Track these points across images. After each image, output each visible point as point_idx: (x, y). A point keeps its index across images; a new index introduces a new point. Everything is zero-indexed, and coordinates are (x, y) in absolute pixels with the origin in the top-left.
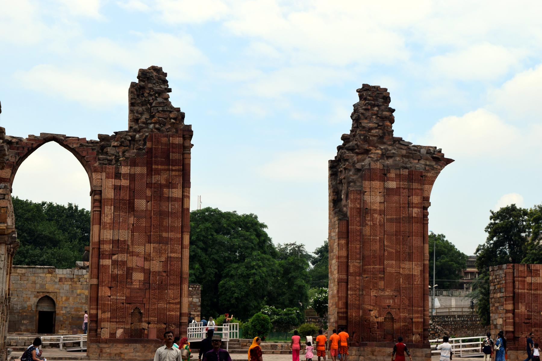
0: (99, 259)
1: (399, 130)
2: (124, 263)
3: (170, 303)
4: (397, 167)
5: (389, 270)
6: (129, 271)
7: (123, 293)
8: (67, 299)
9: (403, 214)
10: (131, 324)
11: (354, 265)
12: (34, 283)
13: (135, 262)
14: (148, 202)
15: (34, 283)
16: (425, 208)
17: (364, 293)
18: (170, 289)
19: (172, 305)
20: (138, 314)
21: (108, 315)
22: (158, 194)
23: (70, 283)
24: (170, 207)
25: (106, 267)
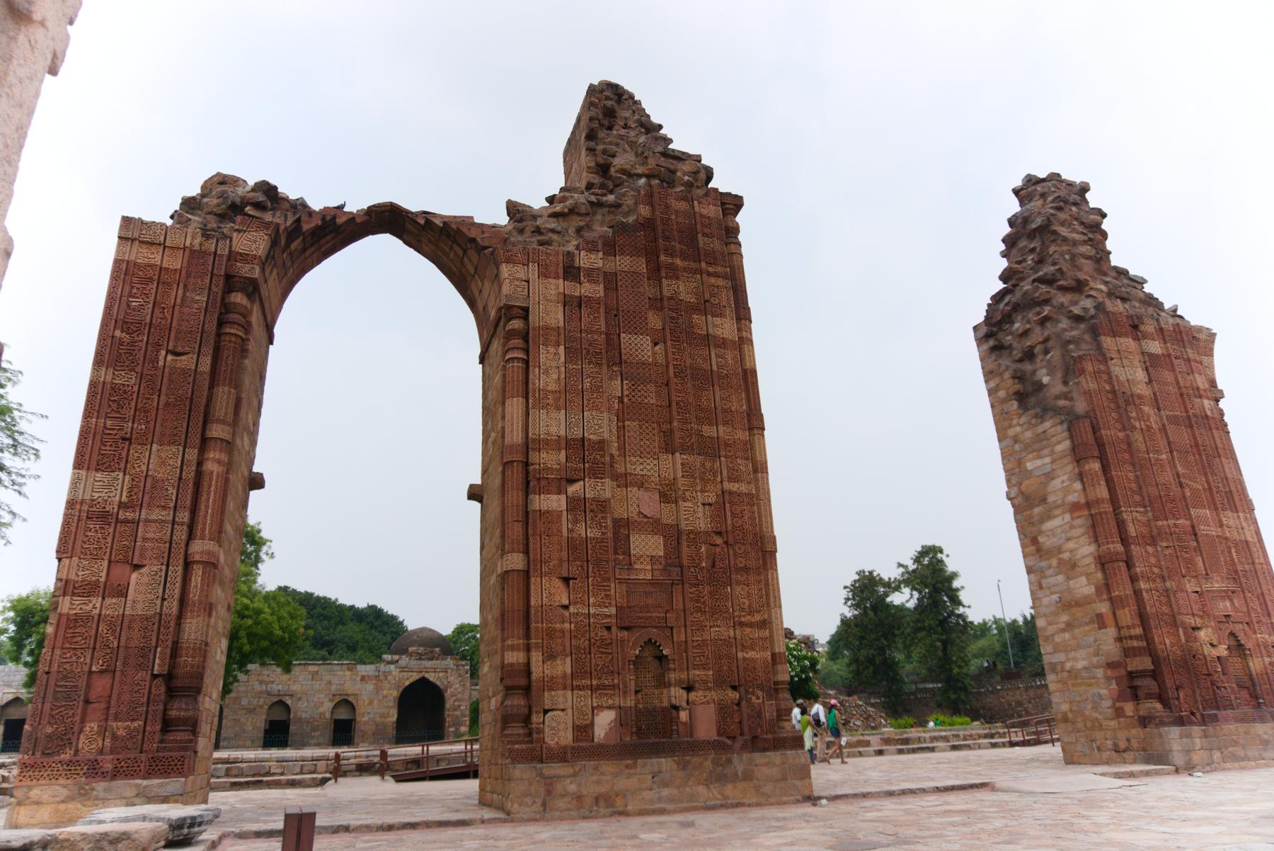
3: (742, 624)
5: (1203, 529)
6: (622, 528)
8: (371, 703)
10: (637, 692)
12: (329, 683)
14: (656, 344)
15: (329, 683)
16: (1217, 401)
18: (738, 583)
19: (748, 630)
21: (564, 666)
22: (680, 327)
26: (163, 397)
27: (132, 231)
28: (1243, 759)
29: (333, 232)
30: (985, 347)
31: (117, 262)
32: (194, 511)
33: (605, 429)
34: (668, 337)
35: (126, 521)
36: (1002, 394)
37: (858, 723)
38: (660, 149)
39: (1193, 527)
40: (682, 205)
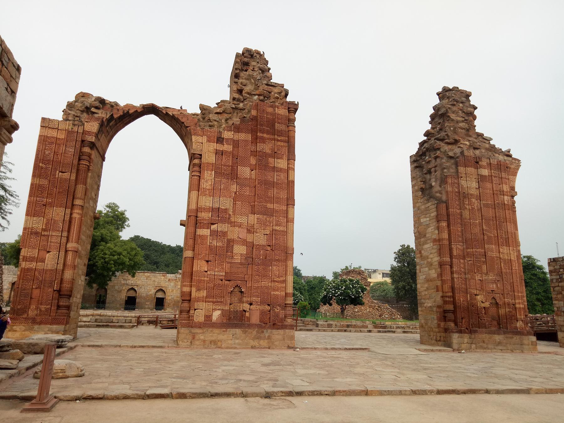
2: (224, 234)
3: (274, 281)
5: (489, 254)
6: (230, 244)
8: (172, 291)
10: (230, 304)
12: (154, 281)
15: (154, 281)
16: (513, 197)
19: (277, 284)
21: (204, 293)
22: (263, 163)
24: (276, 177)
25: (203, 237)
26: (57, 189)
27: (46, 123)
28: (485, 349)
29: (129, 116)
30: (413, 166)
32: (69, 231)
33: (228, 204)
34: (257, 168)
35: (44, 235)
36: (416, 188)
37: (386, 316)
38: (265, 82)
39: (485, 252)
40: (270, 110)
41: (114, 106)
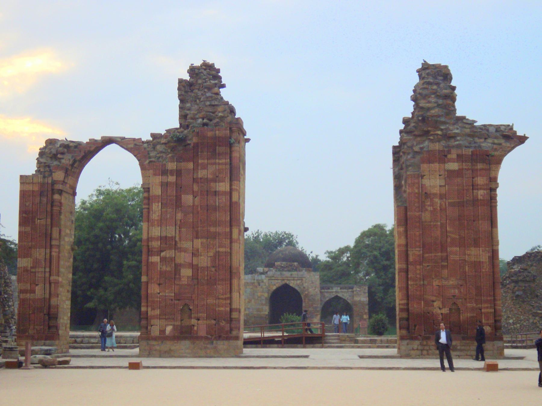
0: (148, 255)
1: (463, 108)
2: (173, 259)
3: (219, 299)
4: (459, 146)
5: (452, 257)
6: (178, 267)
7: (172, 290)
9: (467, 197)
10: (182, 320)
11: (414, 253)
13: (183, 258)
14: (195, 197)
17: (426, 282)
19: (221, 301)
20: (187, 311)
23: (251, 287)
25: (154, 264)
27: (24, 179)
31: (21, 191)
32: (50, 267)
35: (32, 272)
41: (78, 145)
